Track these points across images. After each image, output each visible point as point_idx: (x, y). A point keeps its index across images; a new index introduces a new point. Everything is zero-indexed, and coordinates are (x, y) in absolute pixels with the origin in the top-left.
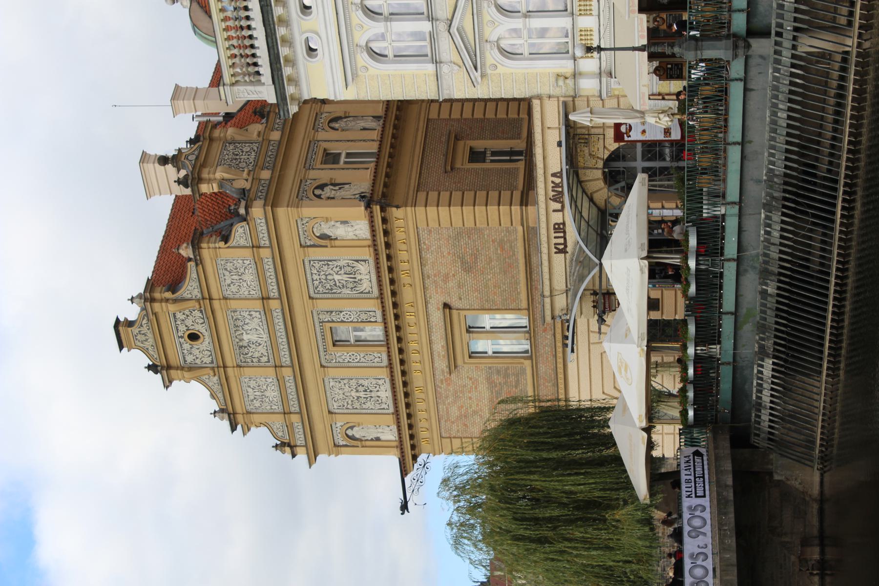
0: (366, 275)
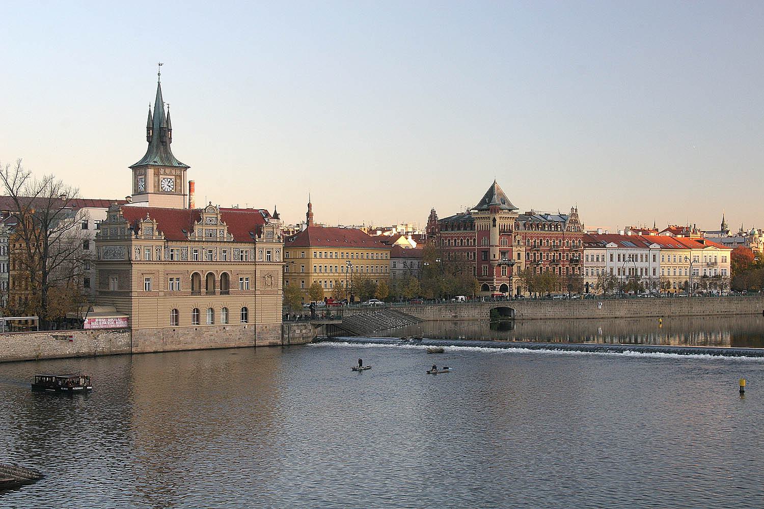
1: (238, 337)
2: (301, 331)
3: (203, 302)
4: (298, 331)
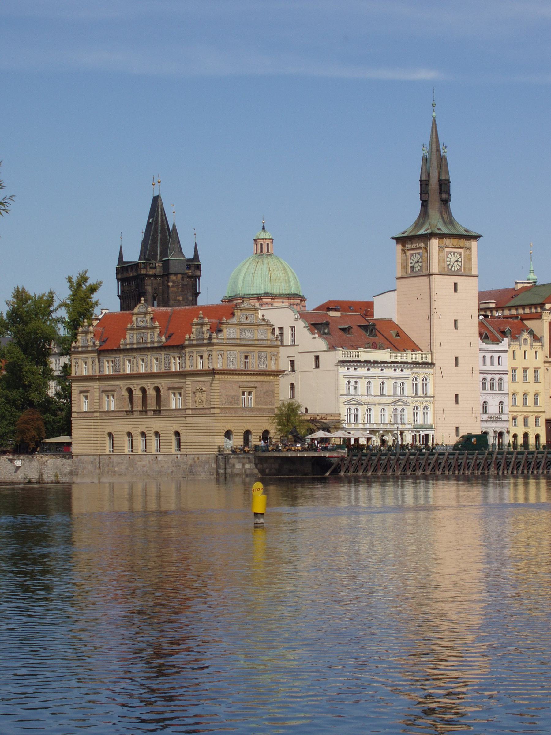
0: (263, 367)
1: (170, 469)
2: (243, 465)
3: (137, 425)
4: (238, 466)
